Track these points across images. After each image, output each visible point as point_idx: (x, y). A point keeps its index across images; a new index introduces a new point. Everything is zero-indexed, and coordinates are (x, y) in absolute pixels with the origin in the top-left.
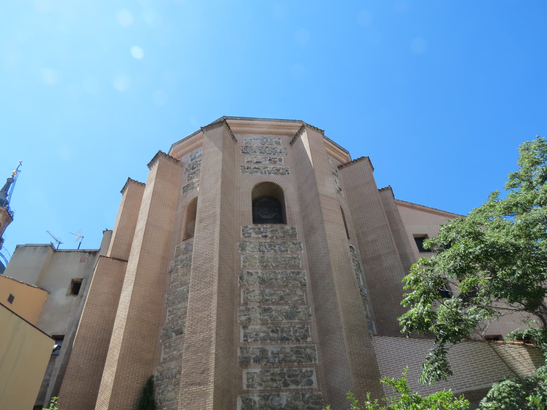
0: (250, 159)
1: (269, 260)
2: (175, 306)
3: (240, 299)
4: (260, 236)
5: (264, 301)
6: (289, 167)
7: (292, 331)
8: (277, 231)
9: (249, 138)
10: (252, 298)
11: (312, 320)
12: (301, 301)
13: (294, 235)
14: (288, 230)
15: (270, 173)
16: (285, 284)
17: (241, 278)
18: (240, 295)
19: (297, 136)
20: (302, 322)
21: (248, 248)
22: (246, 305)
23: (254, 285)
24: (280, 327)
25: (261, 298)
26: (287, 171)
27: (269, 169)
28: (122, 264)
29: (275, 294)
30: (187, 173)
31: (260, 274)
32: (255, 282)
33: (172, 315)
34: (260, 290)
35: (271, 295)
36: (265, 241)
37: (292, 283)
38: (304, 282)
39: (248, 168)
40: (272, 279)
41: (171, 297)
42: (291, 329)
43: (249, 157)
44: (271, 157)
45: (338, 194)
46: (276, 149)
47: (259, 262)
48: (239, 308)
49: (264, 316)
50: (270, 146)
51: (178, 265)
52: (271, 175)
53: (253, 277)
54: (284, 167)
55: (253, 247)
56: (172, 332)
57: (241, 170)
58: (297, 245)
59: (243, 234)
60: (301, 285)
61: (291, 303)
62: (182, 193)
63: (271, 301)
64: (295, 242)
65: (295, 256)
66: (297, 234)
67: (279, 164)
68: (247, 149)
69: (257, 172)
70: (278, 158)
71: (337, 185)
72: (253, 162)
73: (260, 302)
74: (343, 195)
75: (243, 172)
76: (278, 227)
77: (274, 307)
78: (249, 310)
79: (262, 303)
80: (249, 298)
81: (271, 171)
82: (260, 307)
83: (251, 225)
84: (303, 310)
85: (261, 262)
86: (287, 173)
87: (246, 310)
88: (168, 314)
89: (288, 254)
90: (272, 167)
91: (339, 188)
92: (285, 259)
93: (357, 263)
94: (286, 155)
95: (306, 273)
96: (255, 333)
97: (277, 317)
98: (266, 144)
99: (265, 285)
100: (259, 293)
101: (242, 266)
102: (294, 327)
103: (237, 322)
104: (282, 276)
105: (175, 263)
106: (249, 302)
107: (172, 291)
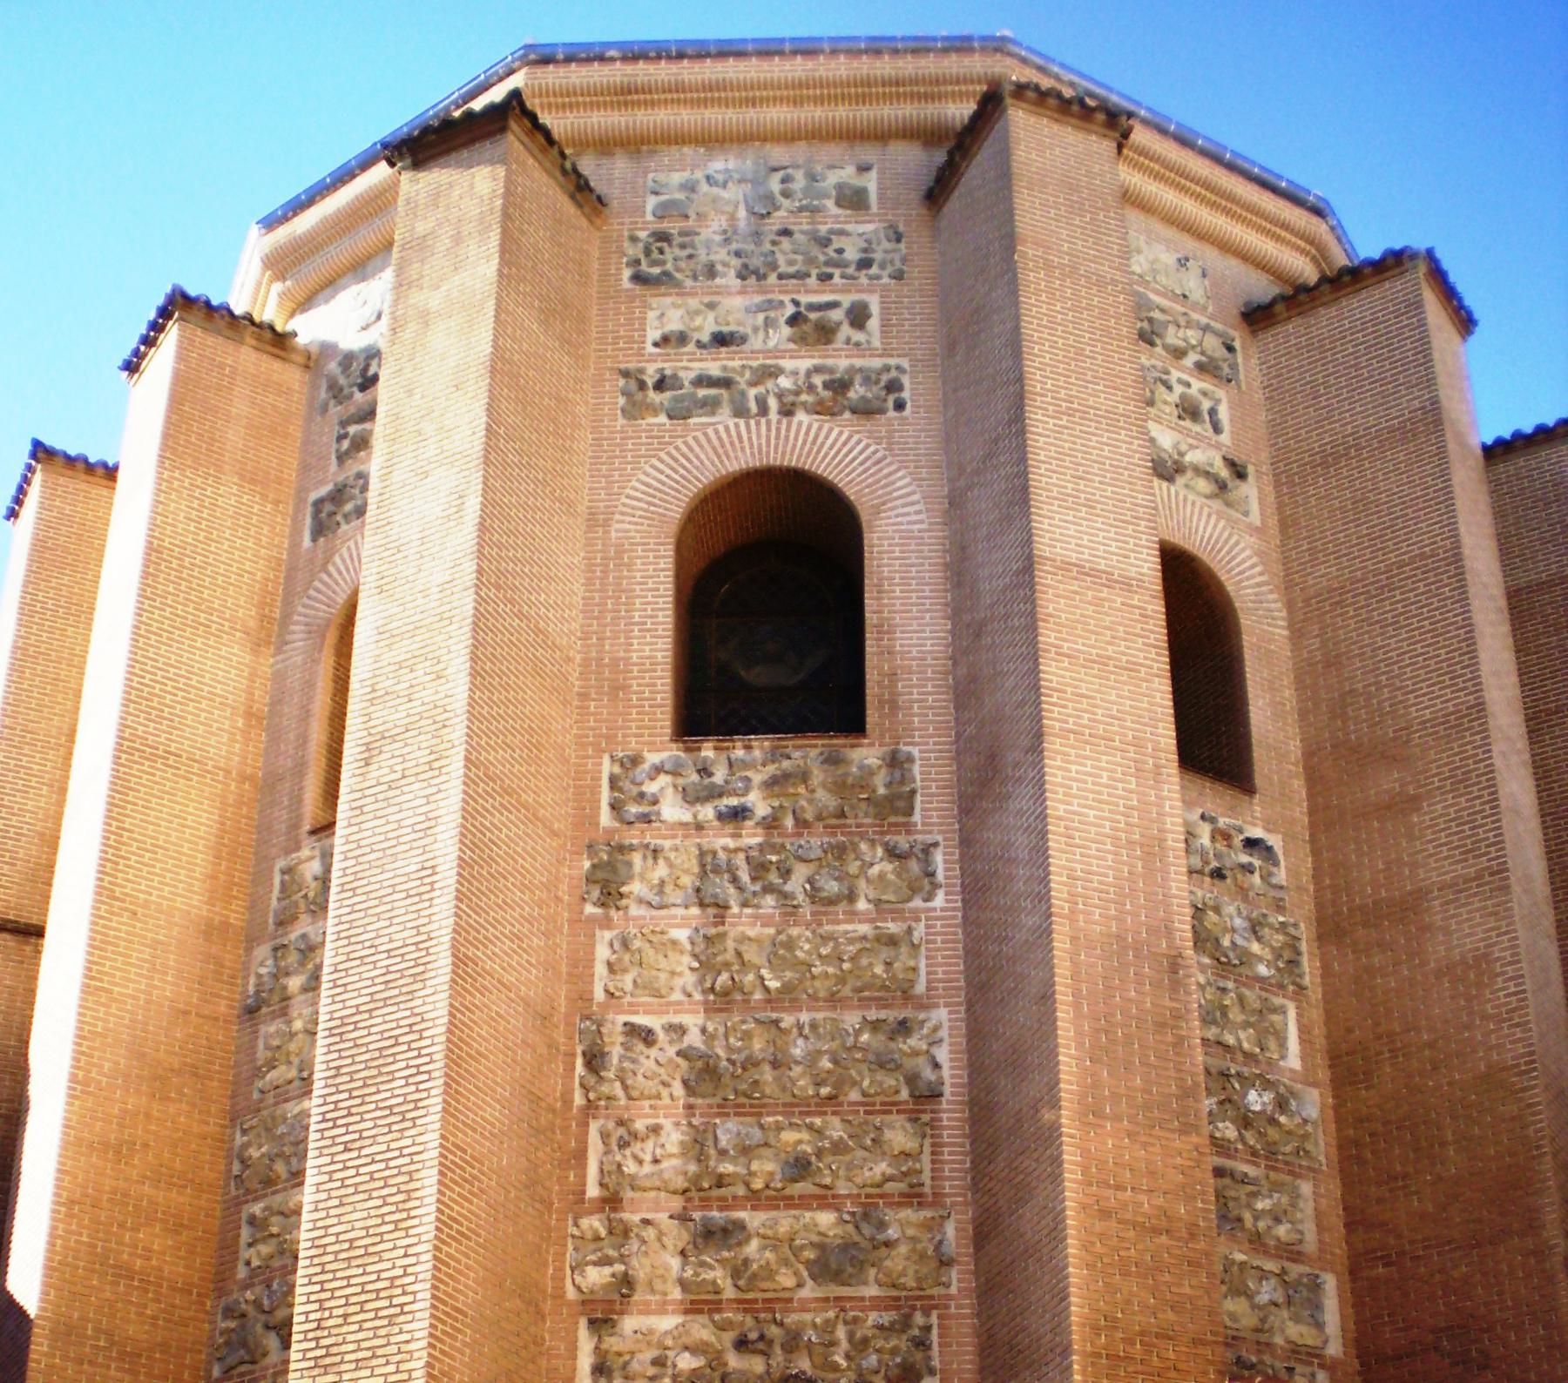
0: (674, 324)
1: (746, 957)
2: (278, 1198)
3: (584, 1176)
4: (707, 812)
5: (706, 1185)
6: (905, 363)
7: (844, 1345)
8: (804, 777)
9: (677, 178)
10: (648, 1168)
11: (953, 1290)
12: (901, 1186)
13: (901, 804)
14: (871, 772)
15: (787, 412)
16: (825, 1091)
17: (595, 1060)
18: (581, 1155)
19: (964, 157)
20: (898, 1299)
21: (635, 887)
22: (614, 1210)
23: (658, 1097)
24: (781, 1324)
25: (693, 1168)
26: (893, 387)
27: (785, 382)
28: (28, 948)
29: (766, 1144)
30: (336, 411)
31: (694, 1039)
32: (665, 1078)
33: (264, 1240)
34: (690, 1124)
35: (746, 1151)
36: (731, 843)
37: (866, 1083)
38: (933, 1078)
39: (660, 385)
40: (756, 1064)
41: (260, 1147)
42: (841, 1333)
43: (674, 305)
44: (805, 299)
45: (1217, 505)
46: (837, 243)
47: (692, 969)
48: (576, 1225)
49: (703, 1264)
50: (802, 224)
51: (287, 974)
52: (796, 420)
53: (653, 1052)
54: (877, 363)
55: (662, 883)
56: (267, 1327)
57: (622, 401)
58: (914, 866)
59: (613, 807)
60: (912, 1095)
61: (848, 1196)
62: (307, 541)
63: (747, 1185)
64: (902, 842)
65: (893, 927)
66: (918, 798)
67: (848, 341)
68: (661, 252)
69: (711, 406)
70: (846, 304)
71: (1218, 446)
72: (696, 336)
73: (685, 1191)
74: (1254, 507)
75: (635, 409)
76: (818, 751)
77: (753, 1219)
78: (621, 1232)
79: (693, 1194)
80: (630, 1167)
81: (797, 393)
82: (683, 1218)
83: (661, 752)
84: (910, 1232)
85: (706, 966)
86: (890, 404)
87: (610, 1233)
88: (245, 1233)
89: (853, 916)
90: (804, 364)
91: (1231, 463)
92: (835, 948)
93: (1278, 939)
94: (898, 276)
95: (946, 1025)
96: (649, 1355)
97: (769, 1272)
98: (777, 208)
99: (717, 1100)
100: (682, 1143)
101: (599, 995)
102: (855, 1320)
103: (559, 1294)
104: (813, 1044)
105: (276, 959)
106: (628, 1194)
107: (265, 1113)
